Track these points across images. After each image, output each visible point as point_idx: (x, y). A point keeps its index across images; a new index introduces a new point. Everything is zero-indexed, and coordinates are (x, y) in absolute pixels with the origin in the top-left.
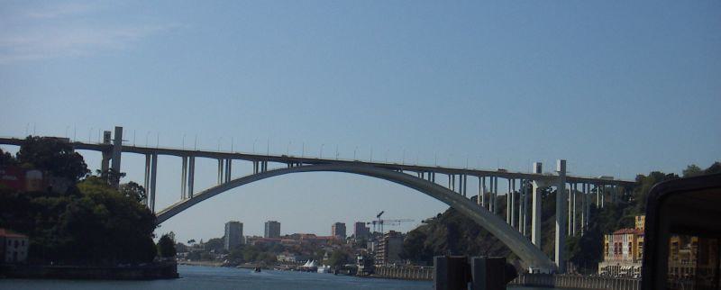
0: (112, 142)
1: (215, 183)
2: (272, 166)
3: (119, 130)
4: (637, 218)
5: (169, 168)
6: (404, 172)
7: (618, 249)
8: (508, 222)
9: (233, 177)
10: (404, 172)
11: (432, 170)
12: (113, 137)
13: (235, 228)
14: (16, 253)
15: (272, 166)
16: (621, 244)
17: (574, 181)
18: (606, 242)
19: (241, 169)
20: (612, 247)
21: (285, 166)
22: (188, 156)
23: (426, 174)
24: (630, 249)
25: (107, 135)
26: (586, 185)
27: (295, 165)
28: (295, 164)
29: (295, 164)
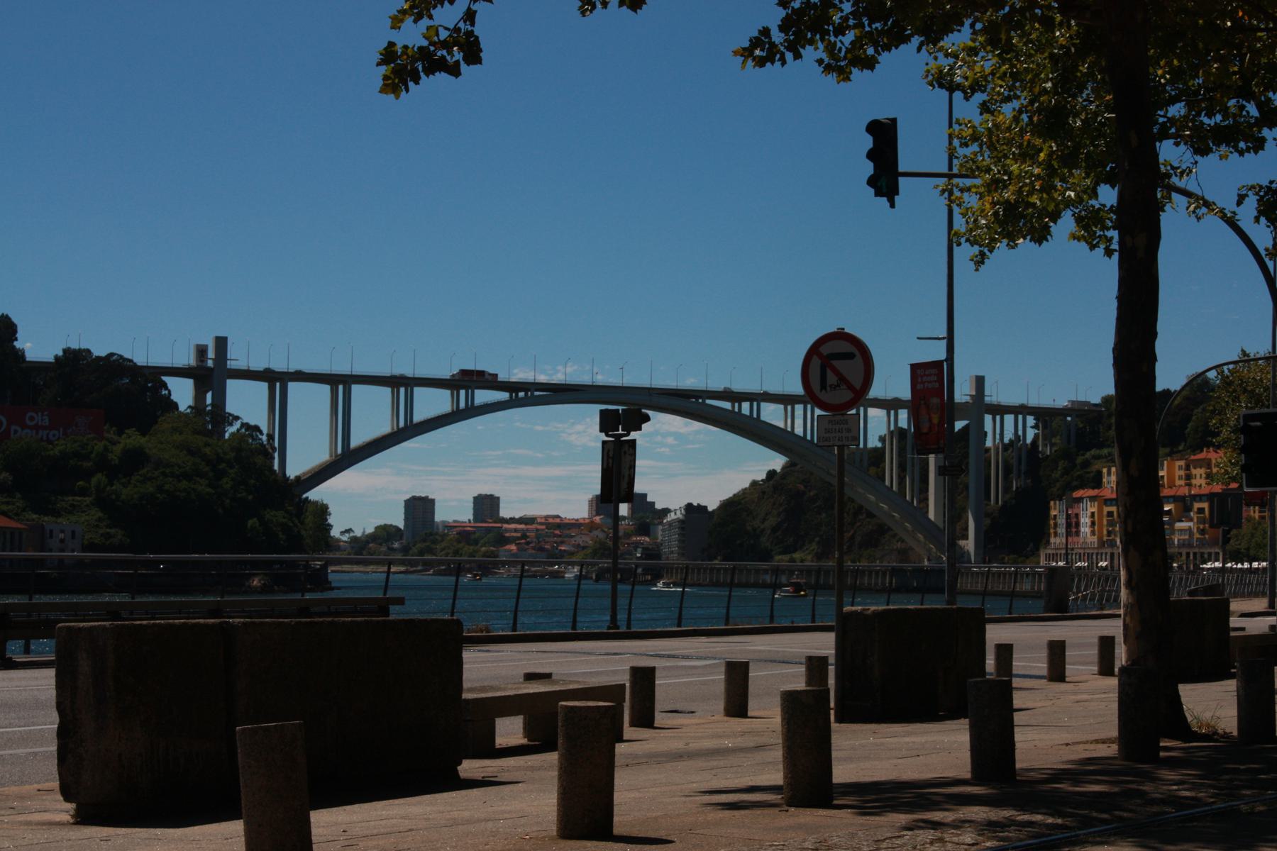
0: (210, 363)
1: (385, 428)
3: (221, 343)
4: (1105, 470)
6: (709, 402)
7: (1073, 526)
8: (887, 483)
9: (418, 417)
10: (709, 402)
12: (211, 354)
13: (419, 508)
15: (483, 396)
16: (1077, 515)
17: (999, 410)
18: (1053, 513)
19: (430, 403)
20: (1062, 521)
21: (503, 396)
22: (340, 383)
23: (746, 407)
24: (1093, 524)
25: (201, 351)
26: (1020, 417)
27: (521, 394)
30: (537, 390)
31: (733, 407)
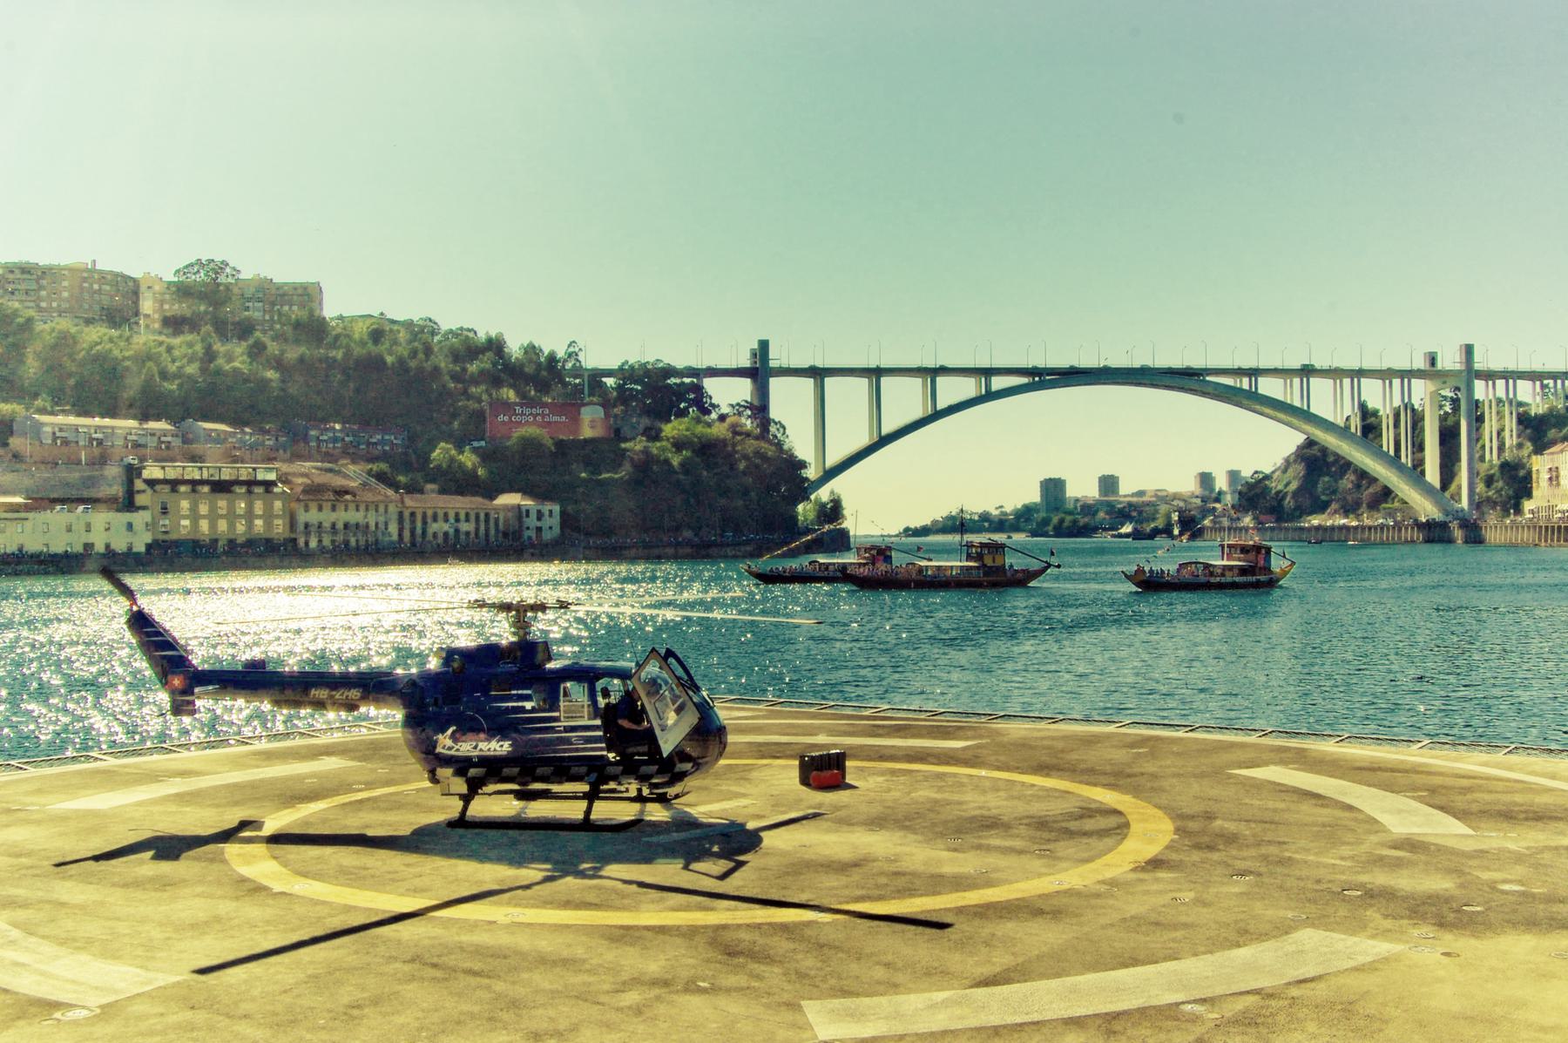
1: (917, 413)
2: (998, 383)
3: (764, 345)
5: (847, 396)
6: (1208, 378)
8: (1385, 448)
10: (1208, 378)
11: (1254, 373)
13: (1053, 488)
14: (539, 529)
15: (998, 383)
16: (1557, 468)
17: (1489, 376)
19: (952, 390)
20: (1545, 476)
21: (1024, 380)
22: (875, 374)
26: (1511, 381)
28: (1042, 378)
29: (1042, 378)
30: (1048, 375)
31: (1236, 382)
